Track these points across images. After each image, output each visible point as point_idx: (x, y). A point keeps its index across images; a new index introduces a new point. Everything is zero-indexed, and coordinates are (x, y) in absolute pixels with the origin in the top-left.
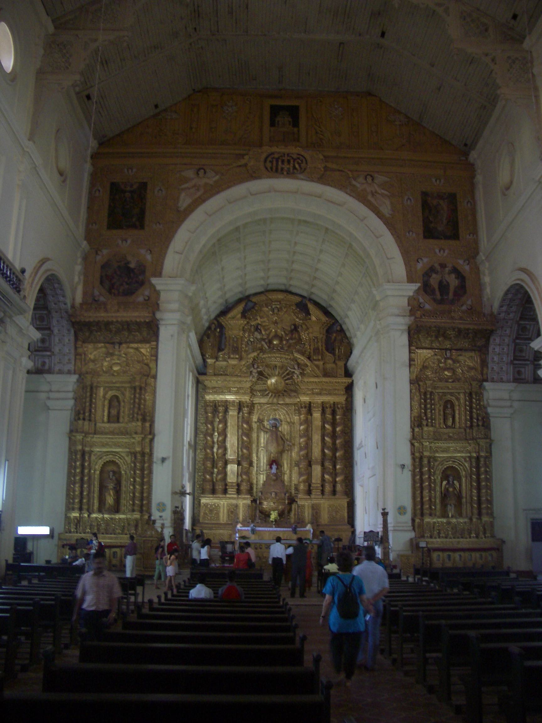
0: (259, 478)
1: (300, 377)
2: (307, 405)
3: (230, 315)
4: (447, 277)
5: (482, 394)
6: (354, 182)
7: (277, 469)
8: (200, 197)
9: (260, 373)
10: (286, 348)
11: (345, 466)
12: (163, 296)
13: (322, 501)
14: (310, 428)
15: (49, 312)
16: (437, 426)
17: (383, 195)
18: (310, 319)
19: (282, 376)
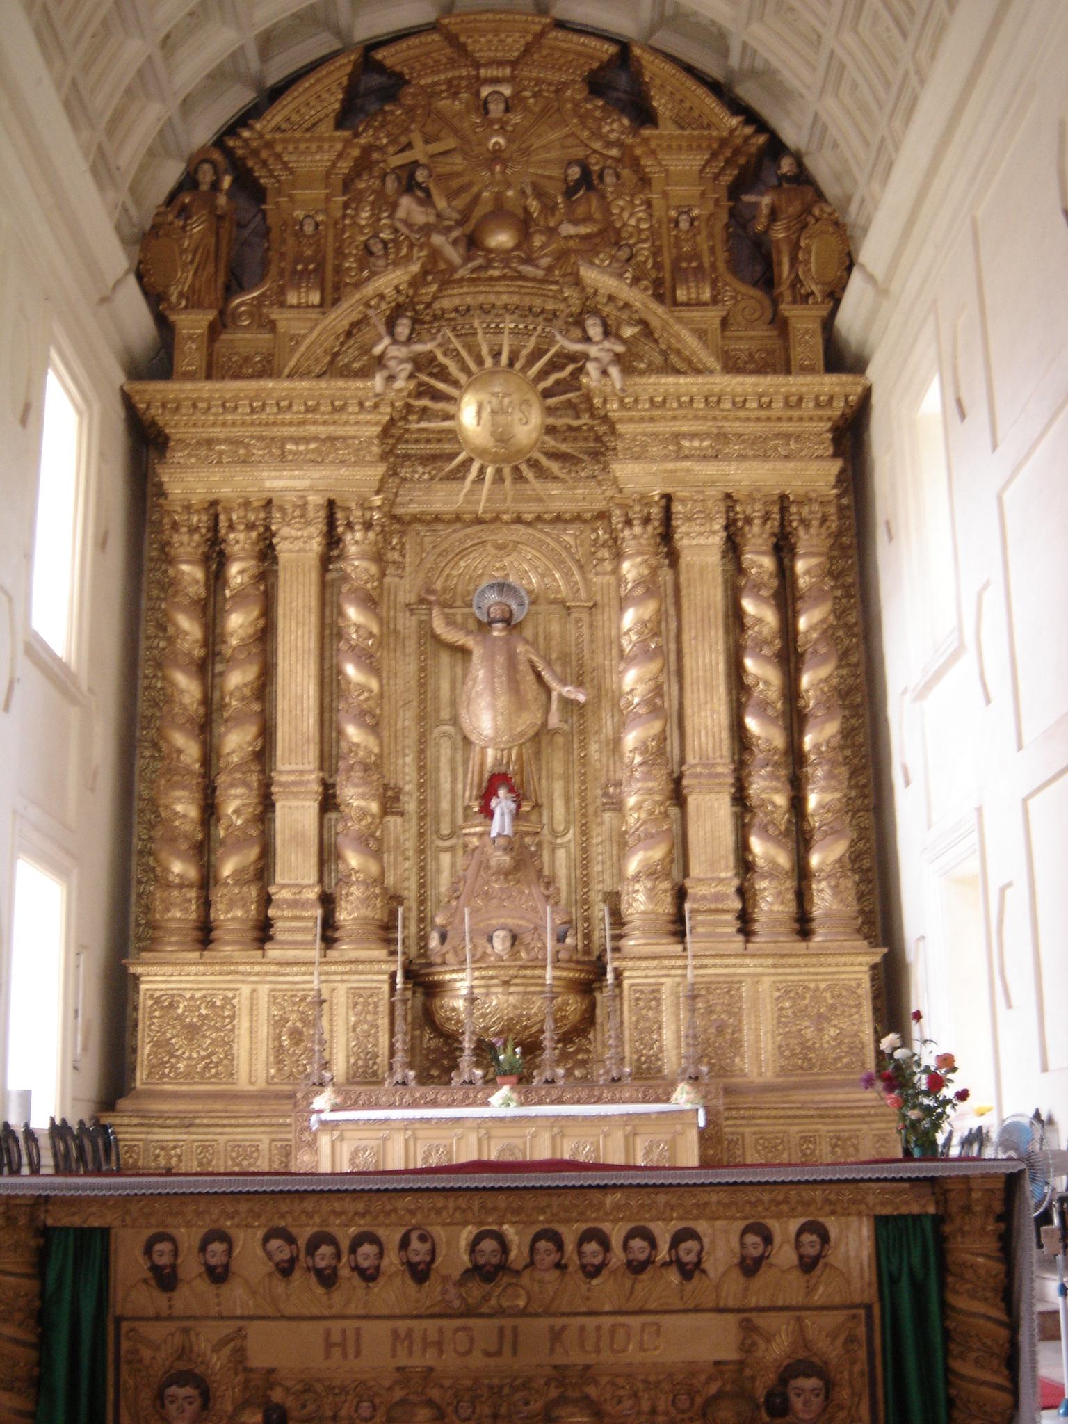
0: (431, 866)
1: (614, 371)
2: (655, 511)
7: (517, 816)
9: (423, 364)
10: (545, 262)
14: (673, 626)
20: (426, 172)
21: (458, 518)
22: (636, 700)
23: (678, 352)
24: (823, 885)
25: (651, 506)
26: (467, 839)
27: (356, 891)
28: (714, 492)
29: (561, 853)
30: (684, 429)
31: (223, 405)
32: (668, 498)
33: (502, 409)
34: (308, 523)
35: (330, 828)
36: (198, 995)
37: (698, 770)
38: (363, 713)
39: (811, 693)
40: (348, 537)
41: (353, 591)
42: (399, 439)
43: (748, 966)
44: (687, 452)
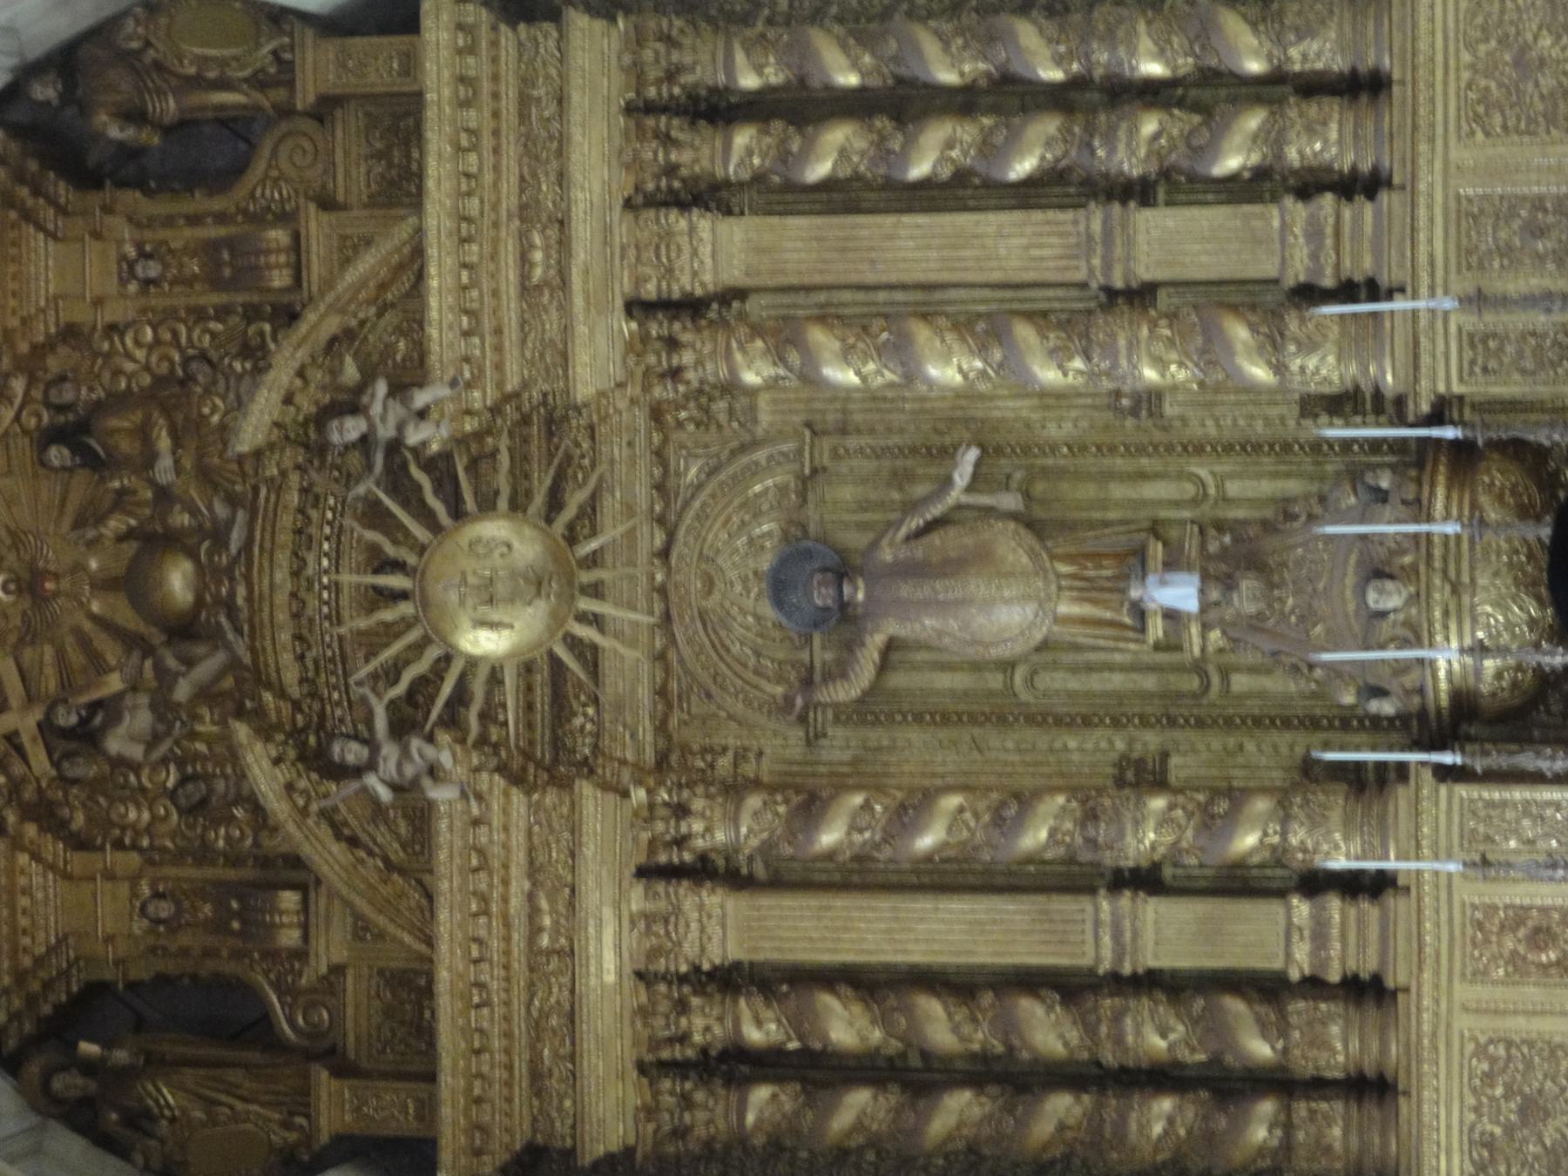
1: (421, 398)
10: (221, 510)
14: (847, 296)
19: (420, 532)
20: (61, 710)
21: (661, 657)
22: (978, 364)
23: (383, 287)
24: (1294, 53)
25: (648, 334)
26: (1210, 649)
28: (622, 229)
29: (1233, 488)
30: (511, 275)
31: (478, 1052)
32: (637, 307)
33: (486, 587)
34: (677, 911)
35: (1189, 877)
36: (1471, 1100)
37: (1096, 262)
38: (998, 820)
39: (967, 68)
40: (700, 843)
41: (791, 837)
42: (528, 756)
43: (1431, 185)
44: (552, 272)
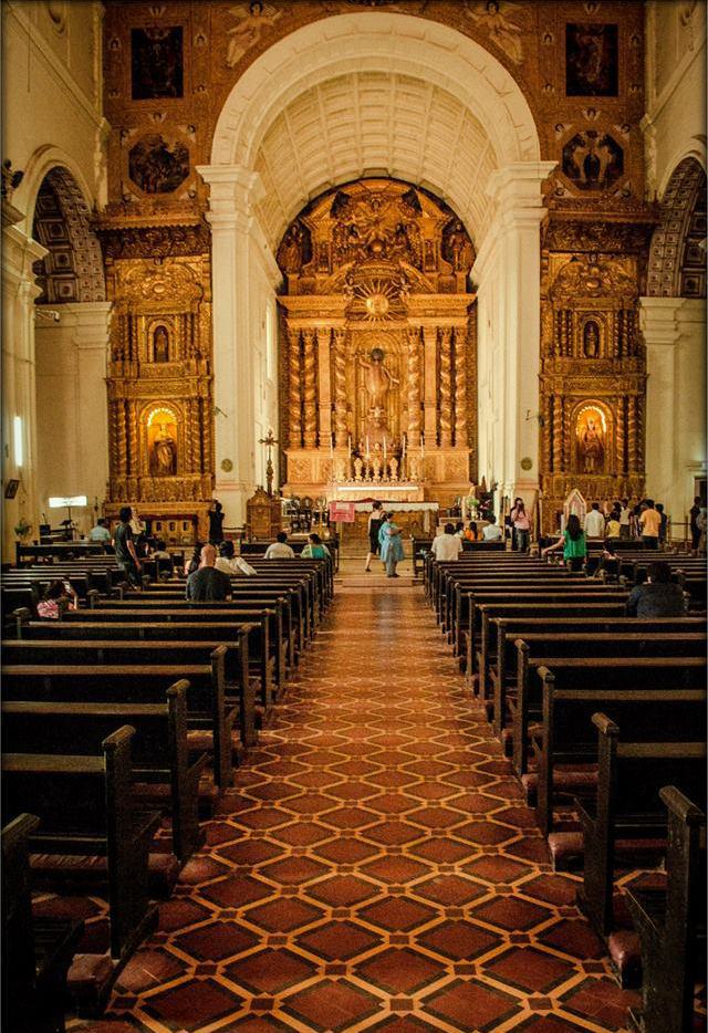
1: (408, 294)
3: (314, 214)
4: (597, 152)
5: (638, 313)
6: (470, 14)
8: (256, 46)
9: (356, 291)
11: (468, 409)
12: (214, 193)
13: (437, 453)
15: (65, 221)
16: (575, 356)
17: (512, 32)
18: (421, 216)
27: (341, 433)
